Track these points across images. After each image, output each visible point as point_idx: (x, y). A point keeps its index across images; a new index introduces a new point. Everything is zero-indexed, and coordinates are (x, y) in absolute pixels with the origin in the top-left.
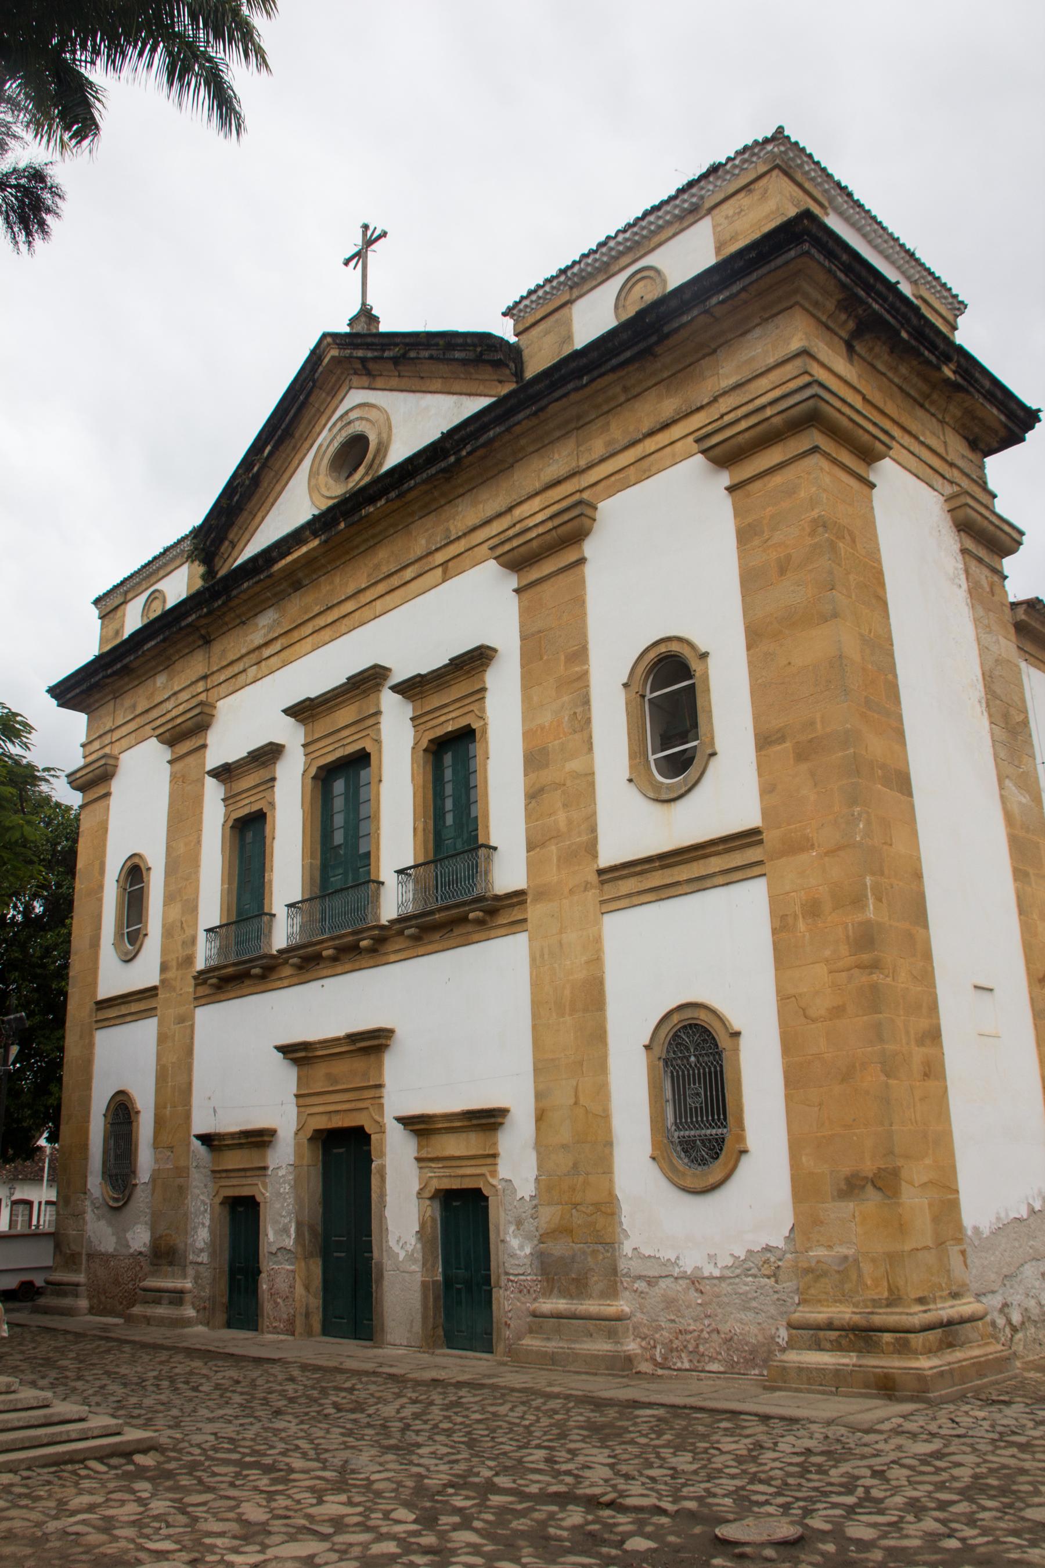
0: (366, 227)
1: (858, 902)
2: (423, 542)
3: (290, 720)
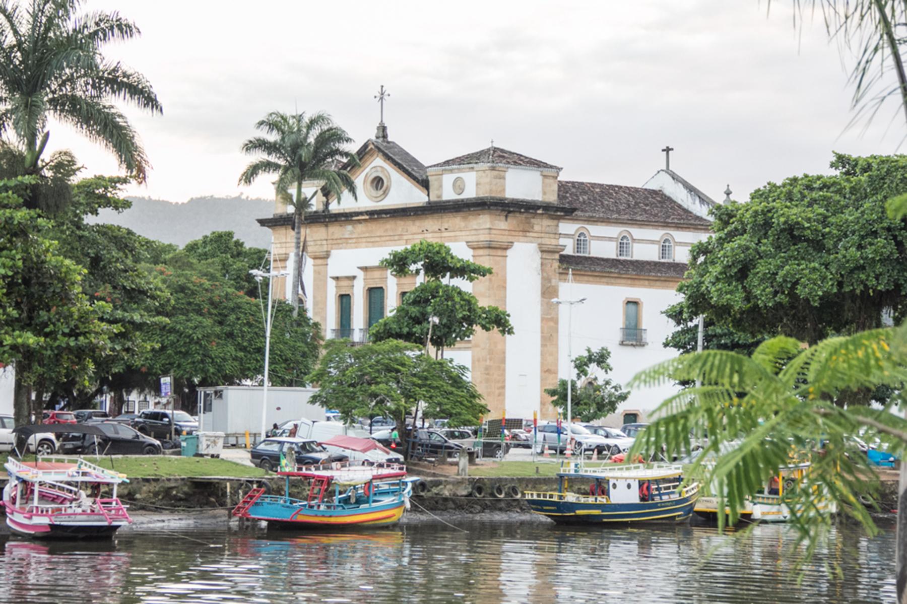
0: (382, 86)
1: (486, 361)
2: (400, 229)
3: (359, 270)
